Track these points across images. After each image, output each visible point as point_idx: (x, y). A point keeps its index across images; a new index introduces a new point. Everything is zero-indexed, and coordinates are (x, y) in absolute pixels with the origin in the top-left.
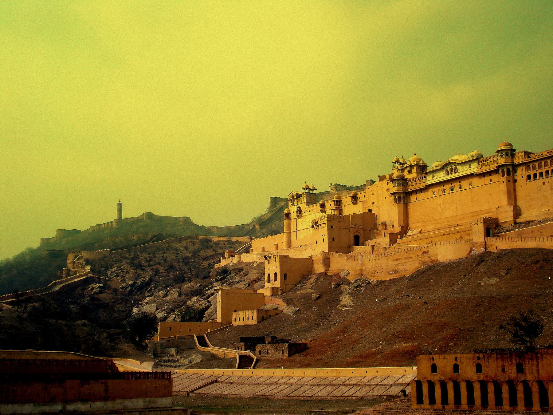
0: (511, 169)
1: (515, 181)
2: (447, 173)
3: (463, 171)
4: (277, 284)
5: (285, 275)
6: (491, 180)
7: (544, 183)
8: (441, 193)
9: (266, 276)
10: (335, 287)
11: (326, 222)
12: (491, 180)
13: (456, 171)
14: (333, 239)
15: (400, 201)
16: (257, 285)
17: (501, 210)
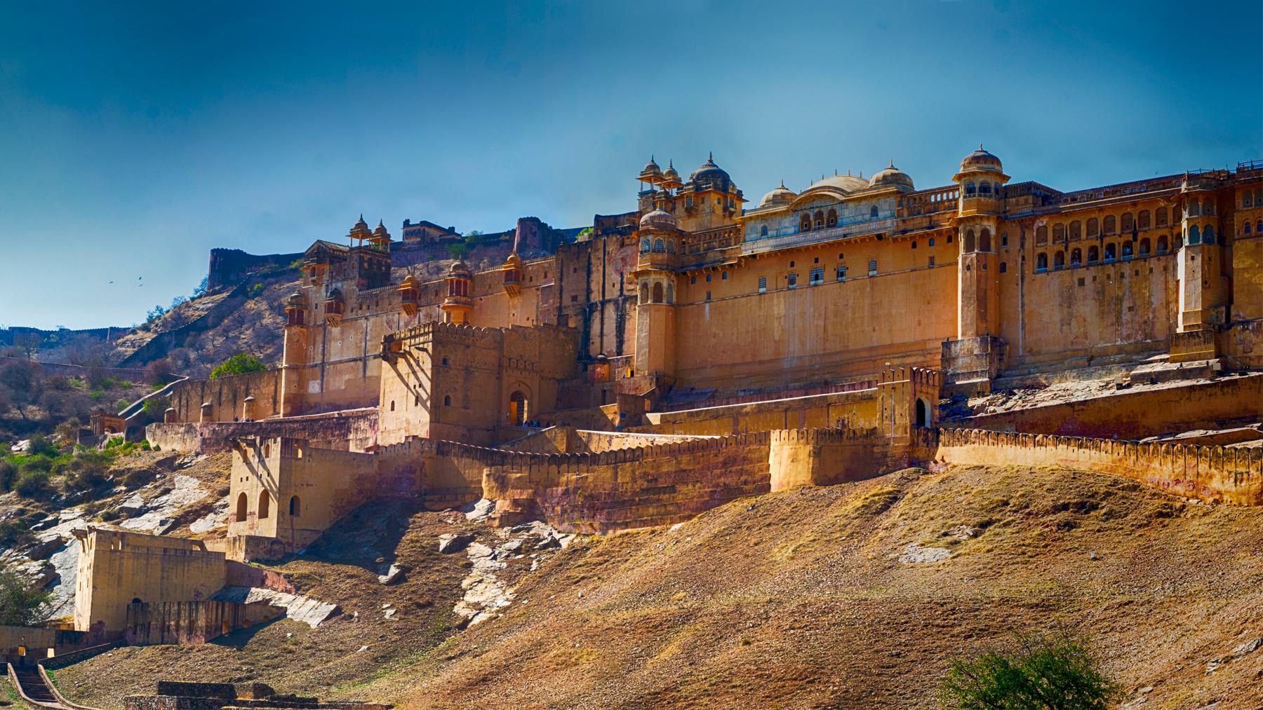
0: (993, 232)
1: (1003, 268)
2: (805, 227)
3: (853, 222)
4: (268, 528)
5: (294, 503)
6: (932, 259)
7: (1082, 282)
8: (783, 283)
9: (232, 500)
10: (448, 549)
11: (430, 347)
12: (932, 259)
13: (833, 221)
14: (447, 400)
15: (658, 298)
16: (199, 527)
17: (956, 349)
